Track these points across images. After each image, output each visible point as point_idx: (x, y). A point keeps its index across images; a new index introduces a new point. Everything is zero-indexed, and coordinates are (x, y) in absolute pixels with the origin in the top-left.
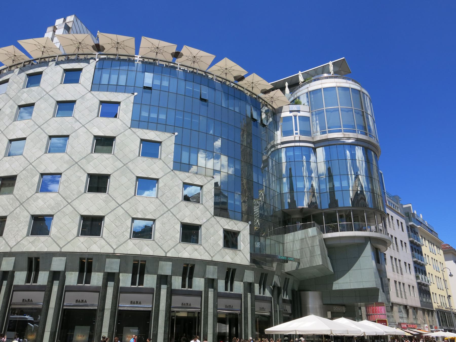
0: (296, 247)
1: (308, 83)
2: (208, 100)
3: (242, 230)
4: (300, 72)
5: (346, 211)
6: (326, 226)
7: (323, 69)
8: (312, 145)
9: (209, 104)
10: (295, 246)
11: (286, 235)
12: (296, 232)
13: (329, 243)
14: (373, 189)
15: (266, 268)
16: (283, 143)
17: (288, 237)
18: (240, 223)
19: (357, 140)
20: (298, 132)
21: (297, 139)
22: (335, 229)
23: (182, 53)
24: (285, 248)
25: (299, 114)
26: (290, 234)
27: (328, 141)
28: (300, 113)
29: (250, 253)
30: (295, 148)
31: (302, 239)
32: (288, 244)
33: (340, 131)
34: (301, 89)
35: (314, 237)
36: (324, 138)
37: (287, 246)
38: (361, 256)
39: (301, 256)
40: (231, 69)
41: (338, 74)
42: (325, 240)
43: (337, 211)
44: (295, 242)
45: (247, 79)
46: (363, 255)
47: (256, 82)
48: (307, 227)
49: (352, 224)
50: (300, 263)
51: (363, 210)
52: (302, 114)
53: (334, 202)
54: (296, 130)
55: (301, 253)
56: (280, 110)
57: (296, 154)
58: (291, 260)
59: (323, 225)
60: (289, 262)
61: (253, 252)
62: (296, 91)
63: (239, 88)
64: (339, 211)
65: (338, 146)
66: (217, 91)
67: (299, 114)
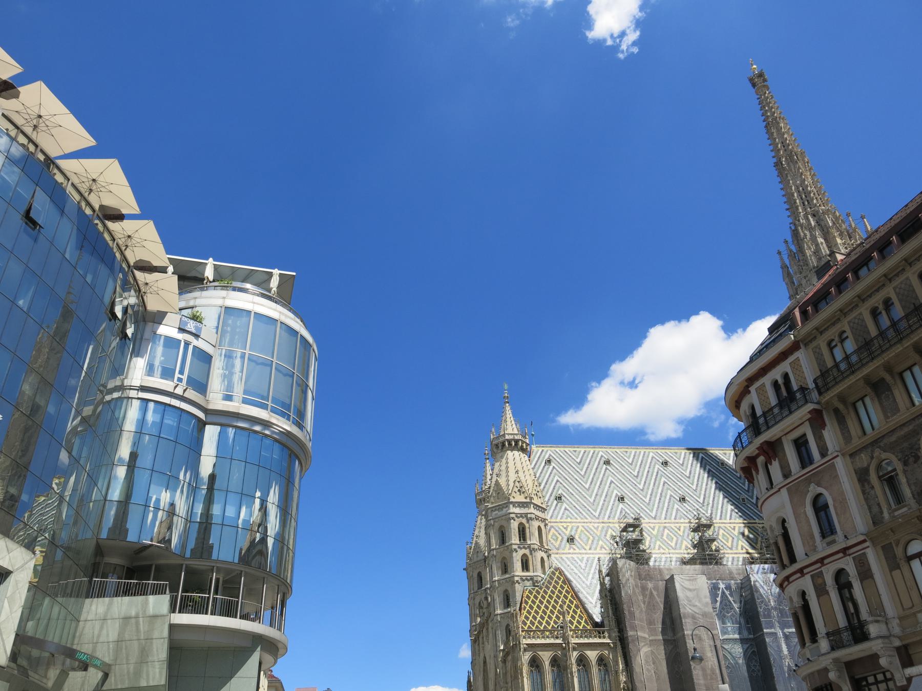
0: (108, 635)
1: (224, 288)
2: (40, 226)
3: (17, 569)
4: (211, 260)
5: (228, 572)
6: (182, 596)
7: (250, 273)
8: (201, 415)
9: (41, 236)
10: (104, 632)
11: (88, 601)
12: (115, 599)
13: (180, 636)
14: (283, 538)
15: (34, 676)
16: (143, 389)
17: (94, 607)
18: (19, 549)
19: (288, 434)
20: (185, 377)
21: (179, 391)
22: (198, 606)
23: (19, 92)
24: (78, 634)
25: (195, 342)
26: (100, 600)
27: (238, 418)
28: (198, 340)
29: (14, 634)
30: (167, 408)
31: (127, 619)
32: (89, 624)
33: (263, 407)
34: (205, 293)
35: (155, 617)
36: (231, 410)
37: (84, 628)
38: (236, 676)
39: (116, 659)
40: (107, 187)
41: (285, 297)
42: (172, 627)
43: (215, 568)
44: (109, 621)
45: (126, 223)
46: (239, 674)
47: (139, 240)
48: (141, 591)
49: (238, 602)
50: (110, 675)
51: (264, 578)
52: (200, 344)
53: (203, 548)
54: (181, 372)
55: (117, 650)
56: (159, 317)
57: (165, 421)
58: (95, 666)
59: (178, 592)
60: (91, 670)
61: (21, 633)
62: (190, 292)
63: (107, 236)
64: (219, 570)
65: (252, 435)
66: (65, 219)
67: (195, 342)
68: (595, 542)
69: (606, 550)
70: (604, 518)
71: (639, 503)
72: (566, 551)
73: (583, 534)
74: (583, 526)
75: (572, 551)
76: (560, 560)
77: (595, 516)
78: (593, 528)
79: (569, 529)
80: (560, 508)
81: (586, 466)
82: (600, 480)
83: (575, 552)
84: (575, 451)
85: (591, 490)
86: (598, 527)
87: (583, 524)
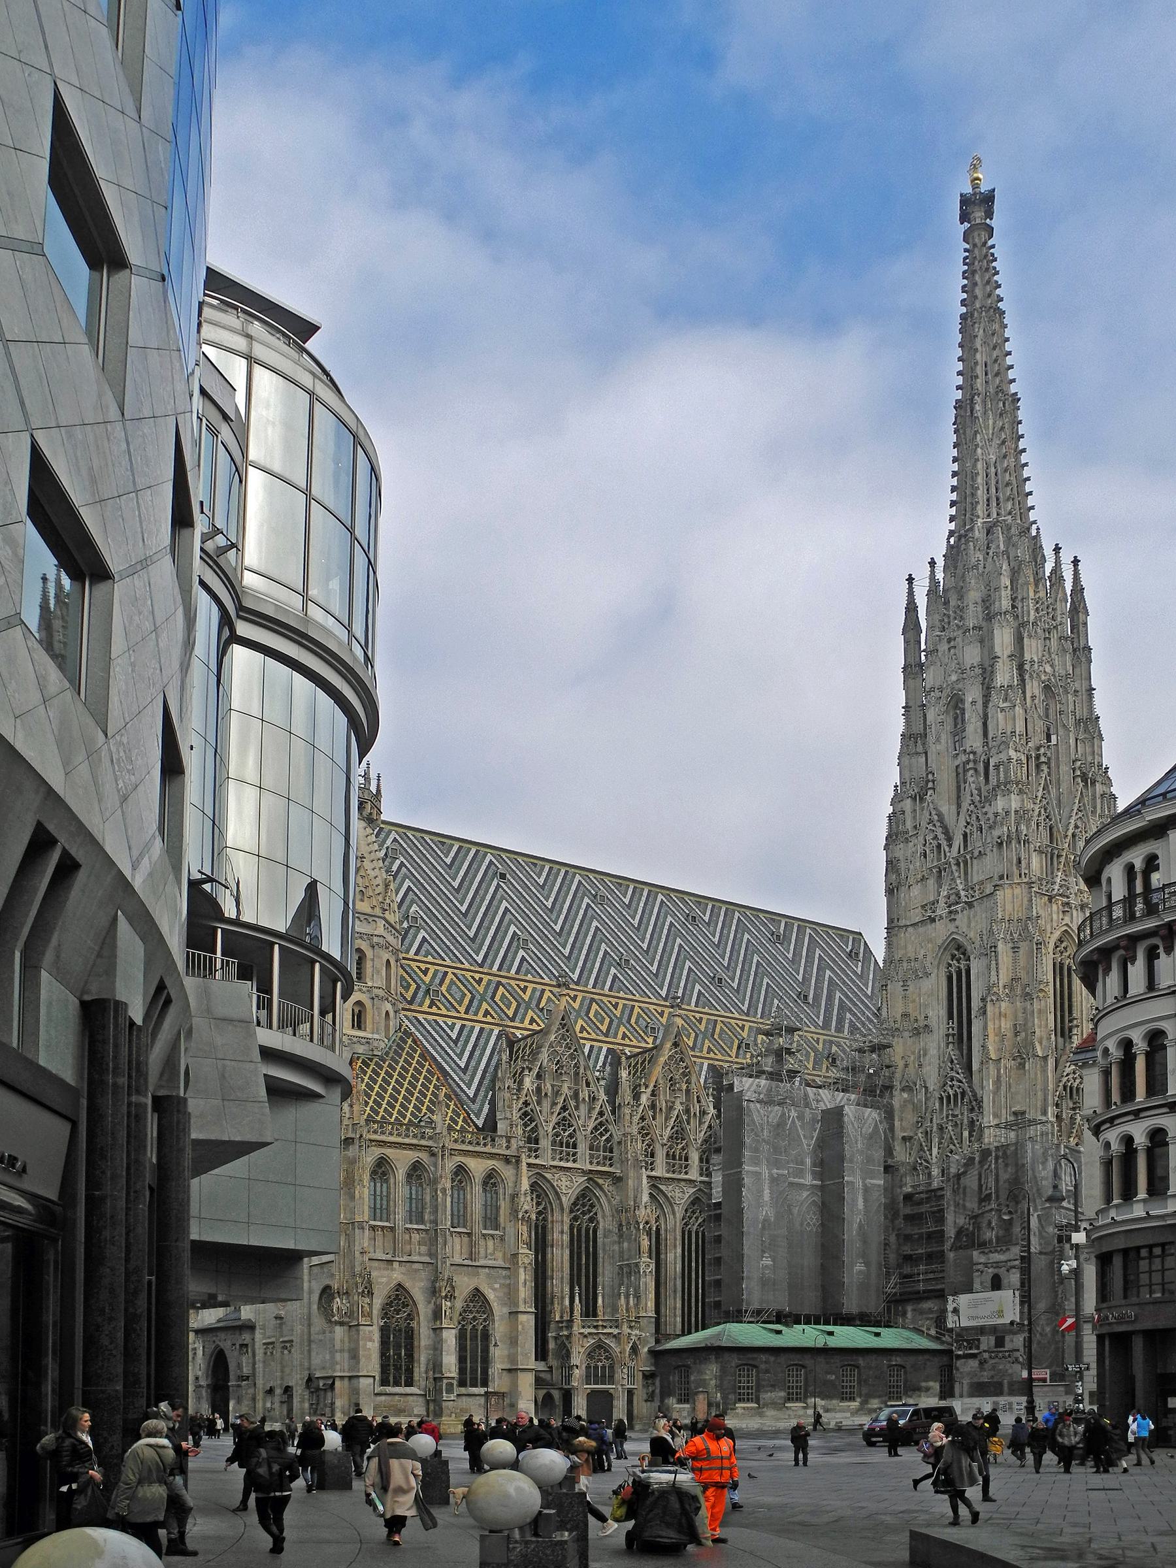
68: (475, 1003)
69: (493, 1018)
70: (491, 968)
71: (552, 954)
72: (425, 1008)
73: (454, 987)
74: (454, 974)
75: (434, 1010)
76: (414, 1021)
77: (475, 961)
78: (472, 980)
79: (430, 974)
80: (415, 937)
81: (462, 873)
82: (486, 902)
83: (439, 1012)
84: (443, 843)
85: (470, 916)
86: (481, 979)
87: (455, 971)
